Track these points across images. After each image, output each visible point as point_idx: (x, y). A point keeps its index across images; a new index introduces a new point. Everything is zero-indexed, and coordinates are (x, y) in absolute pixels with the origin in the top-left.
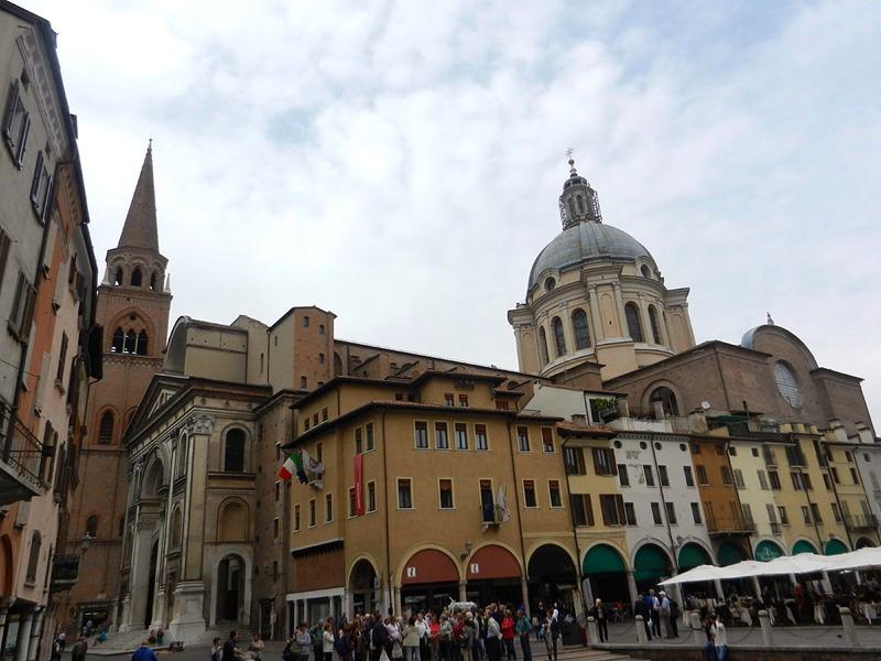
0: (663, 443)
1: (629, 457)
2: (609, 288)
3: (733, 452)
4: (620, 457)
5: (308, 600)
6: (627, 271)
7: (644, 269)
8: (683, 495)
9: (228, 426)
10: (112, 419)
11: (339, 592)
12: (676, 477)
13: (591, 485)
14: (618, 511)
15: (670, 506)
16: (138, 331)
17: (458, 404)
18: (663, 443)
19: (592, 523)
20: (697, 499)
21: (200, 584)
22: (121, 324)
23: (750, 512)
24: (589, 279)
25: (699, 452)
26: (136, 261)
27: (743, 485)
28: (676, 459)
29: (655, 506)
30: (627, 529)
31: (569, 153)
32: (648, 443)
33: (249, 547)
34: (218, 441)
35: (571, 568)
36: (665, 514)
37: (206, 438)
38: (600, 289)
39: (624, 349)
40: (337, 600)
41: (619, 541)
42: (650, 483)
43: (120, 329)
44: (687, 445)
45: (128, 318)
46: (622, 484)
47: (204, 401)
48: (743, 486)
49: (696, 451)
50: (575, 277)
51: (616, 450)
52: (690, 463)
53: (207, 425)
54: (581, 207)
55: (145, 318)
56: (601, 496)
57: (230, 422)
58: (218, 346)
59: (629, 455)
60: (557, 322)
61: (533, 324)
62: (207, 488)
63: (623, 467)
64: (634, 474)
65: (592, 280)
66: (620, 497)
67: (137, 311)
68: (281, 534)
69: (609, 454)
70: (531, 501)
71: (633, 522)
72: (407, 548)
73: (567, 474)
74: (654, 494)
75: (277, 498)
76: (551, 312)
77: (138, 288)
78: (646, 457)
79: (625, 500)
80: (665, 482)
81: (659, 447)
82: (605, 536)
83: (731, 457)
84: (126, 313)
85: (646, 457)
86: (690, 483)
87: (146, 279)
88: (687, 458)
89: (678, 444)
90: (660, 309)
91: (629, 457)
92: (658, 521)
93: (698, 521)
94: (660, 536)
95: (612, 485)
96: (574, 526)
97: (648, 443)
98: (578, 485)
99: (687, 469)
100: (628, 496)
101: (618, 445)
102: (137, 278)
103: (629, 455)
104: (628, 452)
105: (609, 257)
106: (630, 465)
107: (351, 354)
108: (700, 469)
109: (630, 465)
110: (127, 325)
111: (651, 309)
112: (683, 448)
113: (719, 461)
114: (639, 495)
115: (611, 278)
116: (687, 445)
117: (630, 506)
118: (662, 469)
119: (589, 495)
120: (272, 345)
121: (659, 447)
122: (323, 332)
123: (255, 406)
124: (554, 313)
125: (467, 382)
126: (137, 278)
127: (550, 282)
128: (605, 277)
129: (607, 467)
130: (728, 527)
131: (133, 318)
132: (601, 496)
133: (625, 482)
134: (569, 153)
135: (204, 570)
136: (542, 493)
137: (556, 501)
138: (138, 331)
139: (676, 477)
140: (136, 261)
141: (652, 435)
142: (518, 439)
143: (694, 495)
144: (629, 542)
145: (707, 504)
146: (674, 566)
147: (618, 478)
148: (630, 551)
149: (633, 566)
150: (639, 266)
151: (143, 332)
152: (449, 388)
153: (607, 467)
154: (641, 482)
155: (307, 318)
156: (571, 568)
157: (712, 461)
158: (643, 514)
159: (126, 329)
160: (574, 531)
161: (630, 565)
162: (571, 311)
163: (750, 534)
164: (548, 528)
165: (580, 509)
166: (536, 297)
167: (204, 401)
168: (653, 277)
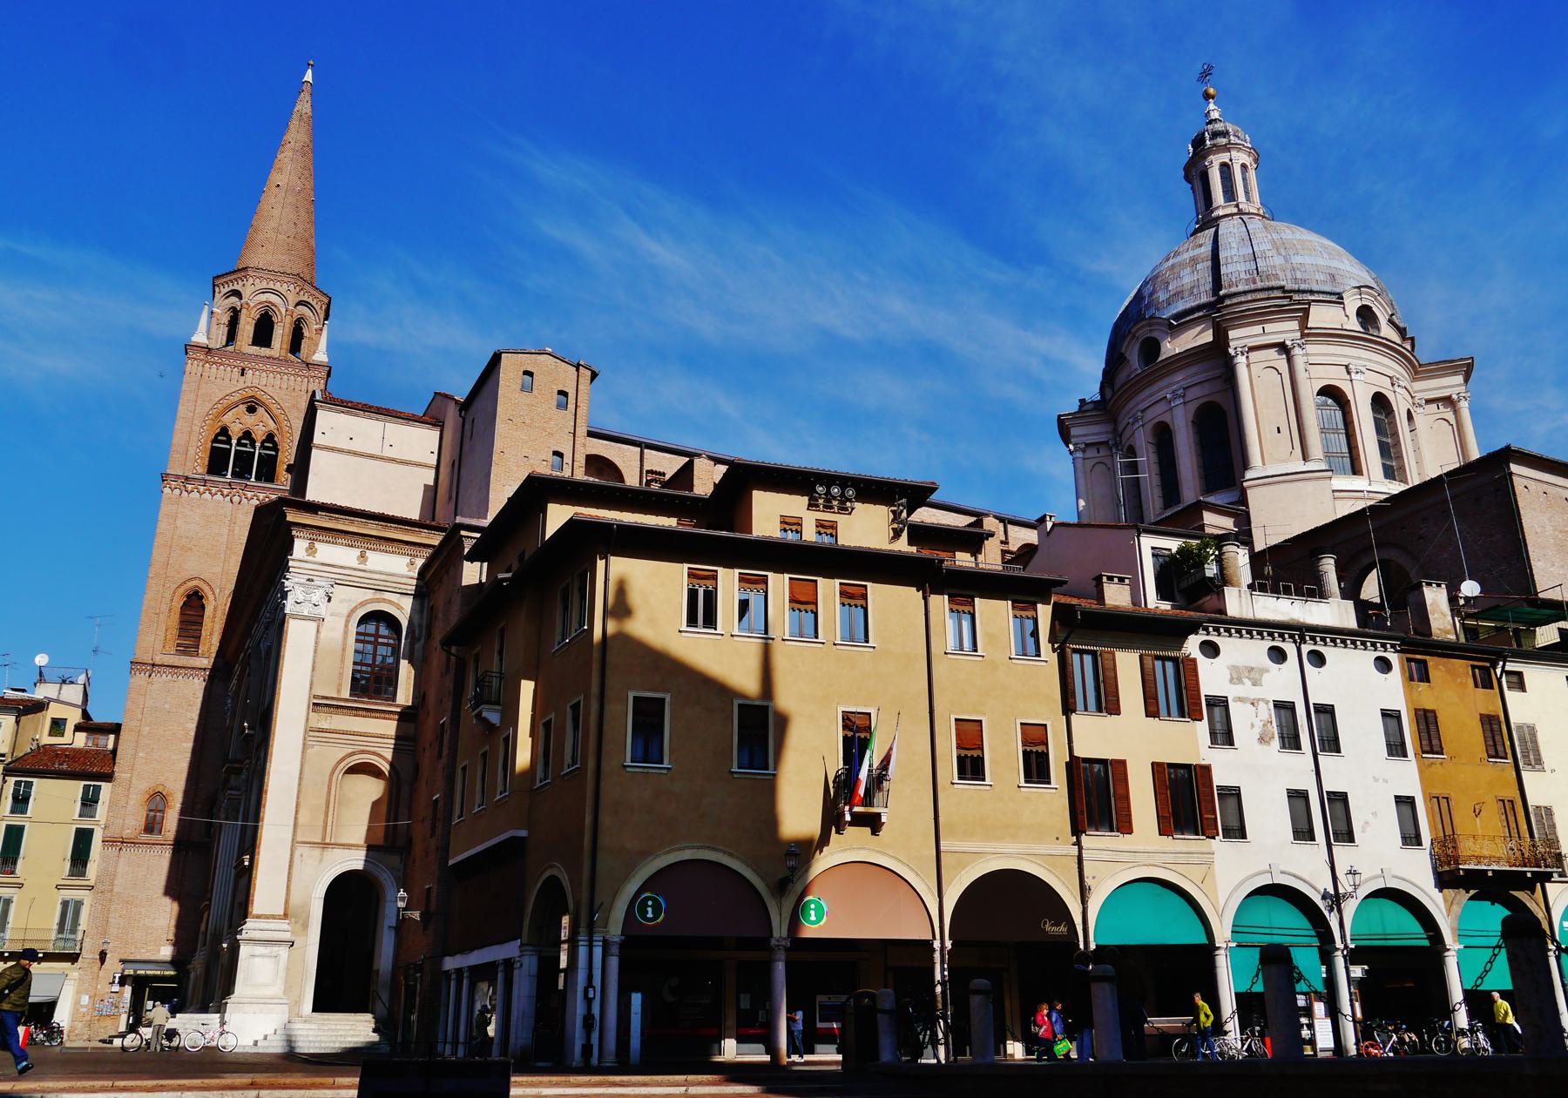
0: (1328, 652)
1: (1236, 679)
2: (1272, 352)
3: (1521, 686)
4: (1212, 678)
5: (471, 968)
6: (1322, 316)
7: (1366, 315)
8: (1372, 776)
9: (362, 604)
10: (203, 607)
11: (510, 950)
12: (1361, 732)
13: (1134, 739)
14: (1191, 802)
15: (1338, 801)
16: (259, 435)
17: (810, 535)
18: (1328, 652)
19: (1126, 827)
20: (1413, 789)
21: (284, 924)
22: (227, 419)
23: (1554, 826)
24: (1232, 334)
25: (1425, 677)
26: (263, 297)
27: (1539, 761)
28: (1361, 685)
29: (1297, 797)
30: (1219, 845)
31: (1205, 74)
32: (1289, 648)
33: (395, 860)
34: (339, 634)
35: (1063, 929)
36: (1325, 817)
37: (313, 625)
38: (1254, 356)
39: (1309, 487)
40: (509, 964)
41: (1196, 873)
42: (1291, 741)
43: (224, 431)
44: (1393, 658)
45: (243, 408)
46: (1214, 741)
47: (311, 550)
48: (1537, 762)
49: (1419, 674)
50: (1200, 336)
51: (1203, 664)
52: (1398, 702)
53: (315, 599)
54: (1230, 194)
55: (273, 407)
56: (1157, 768)
57: (370, 594)
58: (377, 452)
59: (1236, 676)
60: (1163, 436)
61: (1118, 443)
62: (309, 730)
63: (1219, 704)
64: (1248, 721)
65: (1239, 337)
66: (1206, 770)
67: (259, 394)
68: (439, 831)
69: (1186, 673)
70: (971, 767)
71: (1237, 831)
72: (646, 854)
73: (1068, 708)
74: (1296, 769)
75: (440, 756)
76: (1150, 414)
77: (264, 351)
78: (1283, 682)
79: (1219, 779)
80: (1331, 743)
81: (1318, 659)
82: (1158, 859)
83: (1508, 694)
84: (237, 397)
85: (1283, 682)
86: (1396, 748)
87: (281, 335)
88: (1392, 690)
89: (1371, 655)
90: (1400, 404)
91: (1236, 679)
92: (1303, 832)
93: (1411, 838)
94: (1307, 868)
95: (1187, 742)
96: (1077, 830)
97: (1289, 648)
98: (1095, 737)
99: (1390, 716)
100: (1225, 769)
101: (1211, 650)
102: (263, 334)
103: (1236, 676)
104: (1234, 668)
105: (1282, 288)
106: (1240, 699)
107: (646, 468)
108: (1427, 720)
109: (1240, 699)
110: (238, 422)
111: (1380, 403)
112: (1384, 665)
113: (1484, 701)
114: (1258, 771)
115: (1285, 329)
116: (1393, 658)
117: (1233, 795)
118: (1327, 711)
119: (1123, 763)
120: (467, 433)
121: (1318, 659)
122: (562, 406)
123: (420, 562)
124: (1157, 413)
125: (835, 491)
126: (263, 334)
127: (1151, 349)
128: (1269, 327)
129: (1180, 697)
130: (1488, 849)
131: (251, 410)
132: (1157, 768)
133: (1223, 736)
134: (1205, 74)
135: (291, 902)
136: (1003, 753)
137: (1036, 768)
138: (259, 435)
139: (1361, 732)
140: (263, 297)
141: (1300, 632)
142: (950, 624)
143: (1406, 776)
144: (1223, 875)
145: (1442, 804)
146: (1339, 945)
147: (1202, 727)
148: (1222, 902)
149: (1228, 935)
150: (1352, 304)
151: (270, 437)
152: (795, 505)
153: (1180, 697)
154: (1262, 740)
155: (528, 373)
156: (1063, 929)
157: (1454, 694)
158: (1267, 815)
159: (235, 431)
160: (1078, 843)
161: (1223, 933)
162: (1193, 407)
163: (1547, 877)
164: (1022, 831)
165: (1096, 798)
166: (1122, 377)
167: (311, 550)
168: (1387, 331)
